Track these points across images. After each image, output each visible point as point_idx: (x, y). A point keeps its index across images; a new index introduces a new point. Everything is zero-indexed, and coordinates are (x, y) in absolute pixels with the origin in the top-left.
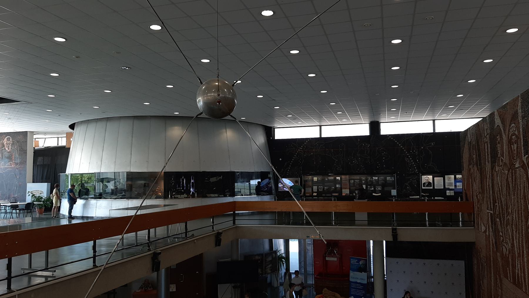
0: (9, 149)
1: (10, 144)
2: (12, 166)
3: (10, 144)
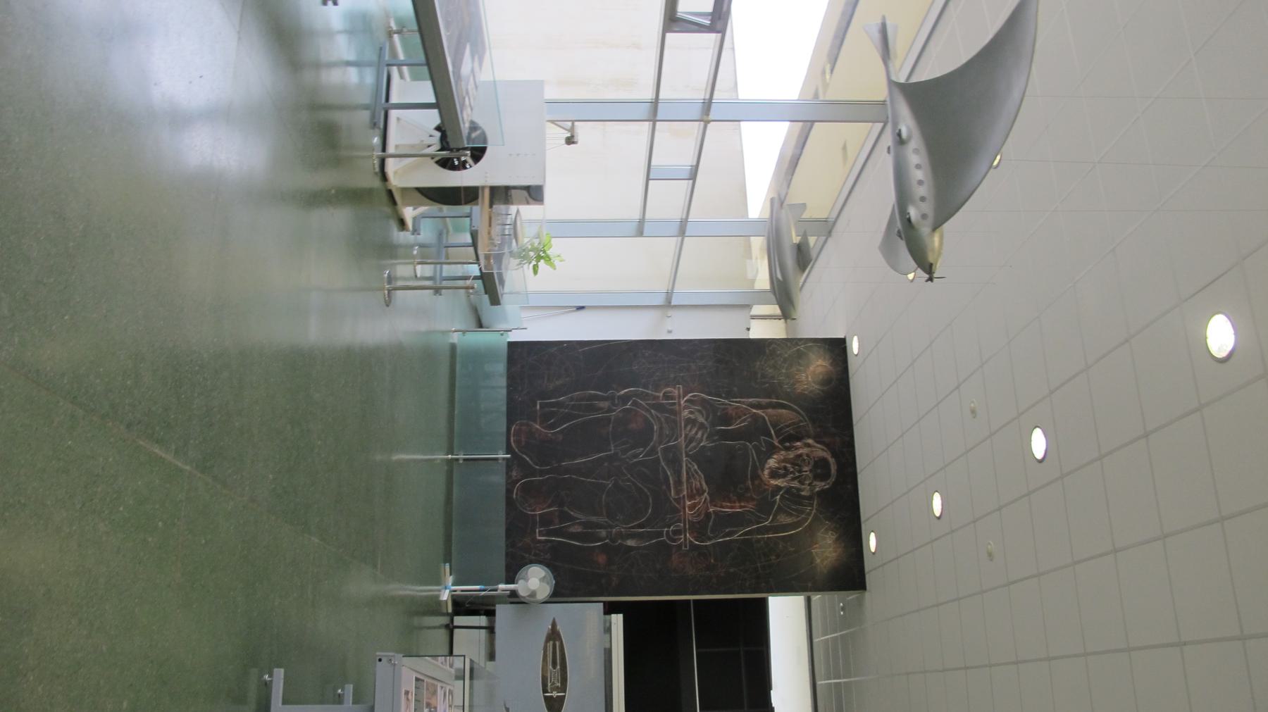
0: (774, 474)
1: (795, 484)
2: (688, 503)
3: (795, 484)
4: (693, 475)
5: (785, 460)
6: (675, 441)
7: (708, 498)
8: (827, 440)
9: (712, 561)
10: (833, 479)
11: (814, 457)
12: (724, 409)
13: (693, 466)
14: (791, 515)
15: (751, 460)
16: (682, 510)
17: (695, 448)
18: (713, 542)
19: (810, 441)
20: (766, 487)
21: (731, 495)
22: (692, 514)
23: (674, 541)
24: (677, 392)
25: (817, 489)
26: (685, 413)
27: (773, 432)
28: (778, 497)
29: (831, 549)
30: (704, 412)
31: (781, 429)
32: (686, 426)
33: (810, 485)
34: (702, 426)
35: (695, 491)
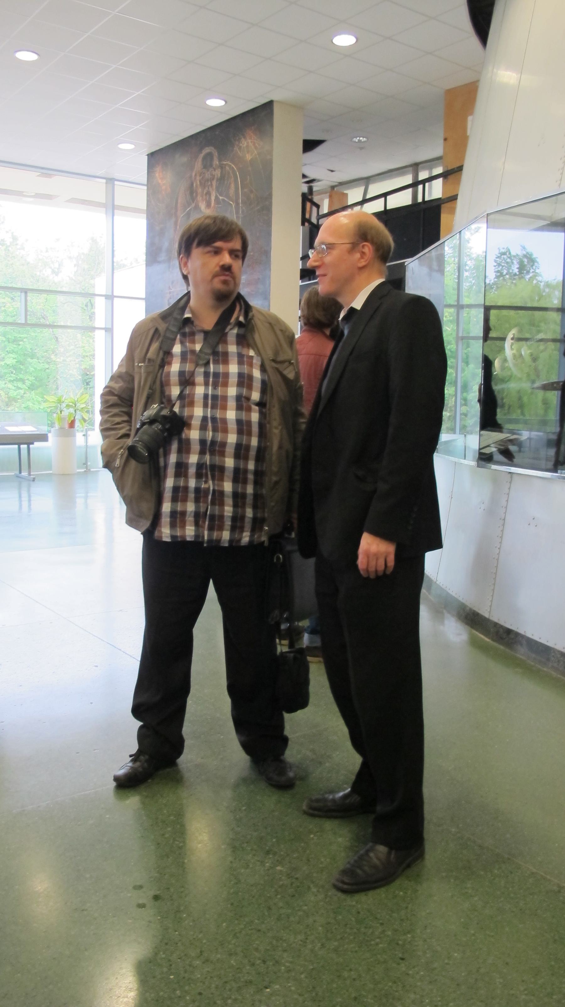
1: (214, 183)
3: (214, 183)
14: (230, 184)
19: (194, 174)
25: (217, 163)
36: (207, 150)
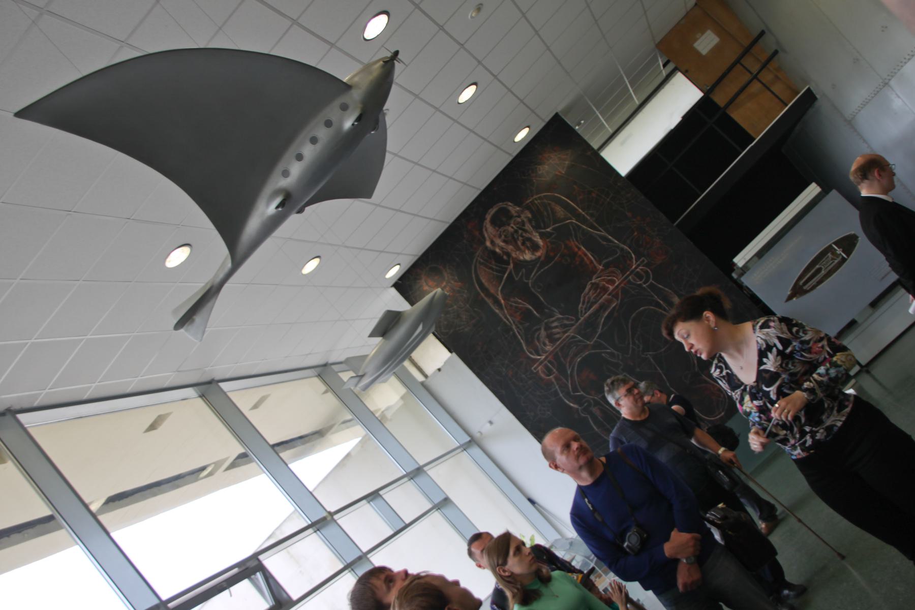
0: (535, 247)
1: (528, 227)
3: (528, 227)
4: (588, 302)
5: (518, 249)
6: (576, 337)
7: (594, 277)
8: (477, 233)
9: (636, 233)
10: (501, 205)
11: (498, 231)
12: (521, 324)
13: (581, 308)
15: (540, 272)
16: (620, 286)
17: (568, 319)
18: (622, 246)
19: (488, 244)
20: (549, 244)
21: (578, 263)
22: (617, 278)
23: (647, 272)
24: (539, 368)
25: (518, 209)
26: (549, 348)
27: (506, 275)
28: (548, 230)
29: (551, 161)
30: (536, 335)
31: (497, 271)
32: (559, 339)
33: (519, 216)
34: (548, 328)
35: (598, 291)
36: (493, 211)
